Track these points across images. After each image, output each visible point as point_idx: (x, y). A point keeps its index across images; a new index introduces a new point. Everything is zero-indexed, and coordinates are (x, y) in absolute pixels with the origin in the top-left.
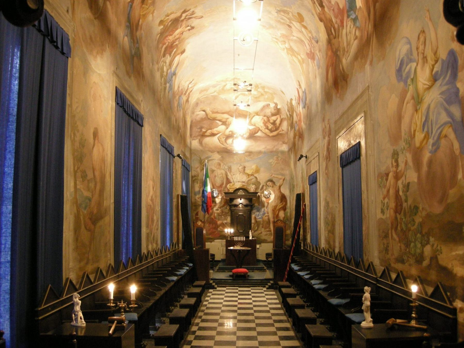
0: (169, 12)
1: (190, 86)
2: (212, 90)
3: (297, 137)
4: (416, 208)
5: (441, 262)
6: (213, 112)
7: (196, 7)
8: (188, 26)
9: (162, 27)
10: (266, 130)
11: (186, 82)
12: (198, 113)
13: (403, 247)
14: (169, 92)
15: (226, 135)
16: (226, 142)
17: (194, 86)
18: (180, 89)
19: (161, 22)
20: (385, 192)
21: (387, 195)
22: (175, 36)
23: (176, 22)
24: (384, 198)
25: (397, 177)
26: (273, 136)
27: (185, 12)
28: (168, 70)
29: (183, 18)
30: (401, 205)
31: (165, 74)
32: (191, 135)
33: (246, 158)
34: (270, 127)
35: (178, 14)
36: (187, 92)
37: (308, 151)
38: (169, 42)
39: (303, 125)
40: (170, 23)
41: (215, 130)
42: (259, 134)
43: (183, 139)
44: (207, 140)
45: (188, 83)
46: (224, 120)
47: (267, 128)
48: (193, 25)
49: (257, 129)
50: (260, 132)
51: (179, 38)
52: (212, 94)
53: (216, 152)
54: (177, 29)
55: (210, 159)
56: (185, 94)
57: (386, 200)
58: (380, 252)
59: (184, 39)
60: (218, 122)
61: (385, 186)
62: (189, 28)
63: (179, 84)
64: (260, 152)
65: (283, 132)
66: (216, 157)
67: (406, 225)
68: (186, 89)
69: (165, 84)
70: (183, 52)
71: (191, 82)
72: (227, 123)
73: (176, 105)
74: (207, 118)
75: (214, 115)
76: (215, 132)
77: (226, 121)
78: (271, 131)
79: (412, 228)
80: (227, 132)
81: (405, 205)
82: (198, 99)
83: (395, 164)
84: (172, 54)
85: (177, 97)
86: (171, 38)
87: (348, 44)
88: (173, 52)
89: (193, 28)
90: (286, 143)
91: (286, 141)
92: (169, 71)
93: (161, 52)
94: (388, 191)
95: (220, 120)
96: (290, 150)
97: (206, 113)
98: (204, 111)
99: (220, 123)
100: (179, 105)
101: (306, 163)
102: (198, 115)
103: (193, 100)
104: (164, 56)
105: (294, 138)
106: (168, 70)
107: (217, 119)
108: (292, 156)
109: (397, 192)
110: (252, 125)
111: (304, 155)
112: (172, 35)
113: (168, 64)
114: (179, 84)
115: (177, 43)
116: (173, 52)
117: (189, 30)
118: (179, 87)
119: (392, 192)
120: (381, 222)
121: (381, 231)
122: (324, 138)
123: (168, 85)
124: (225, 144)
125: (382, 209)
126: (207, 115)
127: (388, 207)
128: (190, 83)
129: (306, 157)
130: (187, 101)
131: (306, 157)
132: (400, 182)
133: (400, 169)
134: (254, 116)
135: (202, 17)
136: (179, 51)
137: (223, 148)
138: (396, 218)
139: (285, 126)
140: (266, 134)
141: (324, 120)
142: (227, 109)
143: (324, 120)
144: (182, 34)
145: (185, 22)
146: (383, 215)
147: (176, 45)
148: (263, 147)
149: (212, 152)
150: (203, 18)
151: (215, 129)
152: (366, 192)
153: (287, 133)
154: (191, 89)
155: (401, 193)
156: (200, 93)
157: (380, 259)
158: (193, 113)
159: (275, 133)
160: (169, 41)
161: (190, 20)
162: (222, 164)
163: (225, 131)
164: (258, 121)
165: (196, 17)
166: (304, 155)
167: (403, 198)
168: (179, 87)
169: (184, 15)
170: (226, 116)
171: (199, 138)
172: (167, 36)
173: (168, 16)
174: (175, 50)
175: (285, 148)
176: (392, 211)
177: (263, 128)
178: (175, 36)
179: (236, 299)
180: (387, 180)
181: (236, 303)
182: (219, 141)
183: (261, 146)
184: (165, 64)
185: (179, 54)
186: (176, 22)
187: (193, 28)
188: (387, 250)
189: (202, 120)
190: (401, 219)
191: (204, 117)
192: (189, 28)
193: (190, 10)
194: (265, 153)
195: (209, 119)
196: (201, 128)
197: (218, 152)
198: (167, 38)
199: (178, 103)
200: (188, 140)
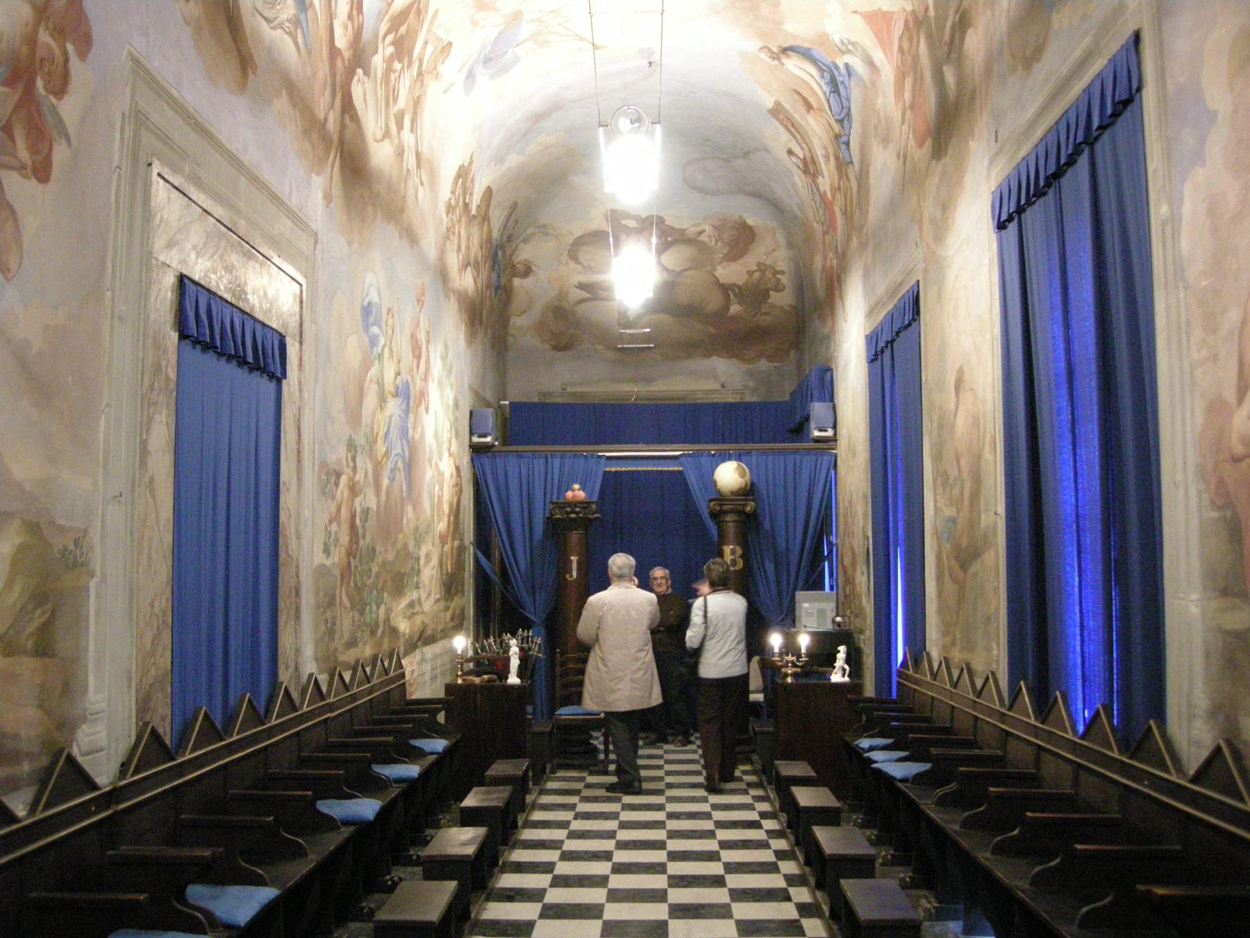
4: (374, 550)
5: (392, 623)
13: (357, 615)
20: (333, 510)
21: (335, 518)
24: (331, 522)
25: (354, 490)
30: (357, 543)
57: (334, 527)
58: (317, 643)
61: (333, 497)
67: (361, 577)
79: (369, 582)
81: (362, 542)
83: (351, 464)
94: (339, 510)
109: (353, 517)
119: (345, 513)
120: (321, 571)
121: (322, 594)
125: (325, 544)
127: (337, 540)
132: (357, 501)
133: (357, 478)
138: (349, 563)
146: (328, 556)
152: (294, 489)
155: (358, 522)
157: (317, 660)
167: (361, 531)
176: (343, 550)
179: (658, 856)
180: (337, 485)
181: (659, 882)
188: (331, 633)
190: (356, 567)
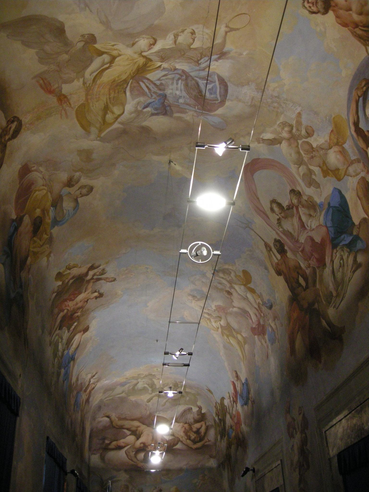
0: (72, 264)
1: (92, 381)
2: (119, 390)
3: (233, 447)
6: (120, 419)
7: (107, 263)
8: (95, 292)
9: (60, 283)
10: (188, 441)
11: (87, 375)
12: (100, 419)
14: (64, 382)
16: (136, 457)
17: (97, 382)
18: (79, 382)
19: (59, 275)
22: (77, 304)
23: (80, 281)
26: (197, 449)
27: (92, 268)
28: (64, 350)
29: (89, 277)
31: (60, 354)
32: (90, 448)
33: (162, 478)
35: (83, 270)
36: (87, 389)
37: (255, 463)
38: (68, 310)
39: (244, 428)
40: (71, 281)
41: (122, 442)
42: (179, 446)
43: (79, 451)
44: (111, 455)
45: (89, 376)
46: (134, 429)
47: (189, 438)
48: (102, 291)
51: (82, 307)
52: (118, 396)
54: (80, 293)
55: (115, 479)
56: (85, 391)
59: (88, 310)
60: (125, 431)
62: (96, 294)
63: (78, 375)
64: (180, 470)
66: (123, 477)
68: (87, 383)
69: (60, 368)
70: (86, 330)
71: (94, 376)
72: (138, 432)
73: (72, 402)
74: (112, 425)
75: (120, 423)
76: (123, 444)
77: (137, 430)
80: (138, 444)
82: (101, 401)
84: (72, 329)
85: (75, 392)
86: (71, 305)
87: (340, 284)
88: (73, 327)
89: (101, 295)
90: (214, 457)
91: (214, 455)
92: (66, 352)
93: (56, 322)
95: (128, 429)
96: (221, 465)
97: (110, 419)
98: (108, 417)
99: (128, 432)
100: (76, 403)
101: (252, 479)
102: (101, 421)
103: (96, 400)
104: (60, 328)
105: (229, 446)
106: (64, 350)
107: (125, 427)
108: (226, 474)
111: (251, 468)
112: (71, 300)
113: (65, 341)
114: (78, 375)
115: (79, 314)
116: (73, 327)
117: (96, 298)
118: (77, 379)
122: (292, 436)
123: (63, 371)
124: (135, 460)
126: (111, 422)
128: (93, 377)
129: (254, 470)
130: (88, 401)
131: (254, 470)
135: (115, 280)
136: (81, 327)
137: (132, 465)
139: (212, 433)
140: (187, 445)
141: (288, 411)
142: (137, 413)
143: (288, 411)
144: (87, 301)
145: (91, 284)
147: (78, 316)
149: (119, 470)
150: (116, 282)
151: (122, 441)
153: (215, 444)
154: (93, 386)
156: (104, 393)
158: (94, 419)
159: (199, 445)
160: (69, 309)
161: (98, 282)
162: (130, 487)
163: (135, 443)
165: (107, 278)
166: (251, 468)
168: (77, 379)
169: (91, 273)
170: (136, 423)
172: (66, 300)
173: (70, 269)
174: (76, 324)
175: (212, 463)
177: (184, 439)
178: (77, 304)
183: (182, 463)
184: (60, 341)
185: (80, 332)
186: (80, 281)
187: (101, 295)
189: (105, 428)
191: (108, 425)
192: (96, 294)
193: (100, 266)
195: (115, 427)
196: (104, 439)
197: (126, 471)
198: (66, 303)
199: (76, 401)
200: (86, 453)
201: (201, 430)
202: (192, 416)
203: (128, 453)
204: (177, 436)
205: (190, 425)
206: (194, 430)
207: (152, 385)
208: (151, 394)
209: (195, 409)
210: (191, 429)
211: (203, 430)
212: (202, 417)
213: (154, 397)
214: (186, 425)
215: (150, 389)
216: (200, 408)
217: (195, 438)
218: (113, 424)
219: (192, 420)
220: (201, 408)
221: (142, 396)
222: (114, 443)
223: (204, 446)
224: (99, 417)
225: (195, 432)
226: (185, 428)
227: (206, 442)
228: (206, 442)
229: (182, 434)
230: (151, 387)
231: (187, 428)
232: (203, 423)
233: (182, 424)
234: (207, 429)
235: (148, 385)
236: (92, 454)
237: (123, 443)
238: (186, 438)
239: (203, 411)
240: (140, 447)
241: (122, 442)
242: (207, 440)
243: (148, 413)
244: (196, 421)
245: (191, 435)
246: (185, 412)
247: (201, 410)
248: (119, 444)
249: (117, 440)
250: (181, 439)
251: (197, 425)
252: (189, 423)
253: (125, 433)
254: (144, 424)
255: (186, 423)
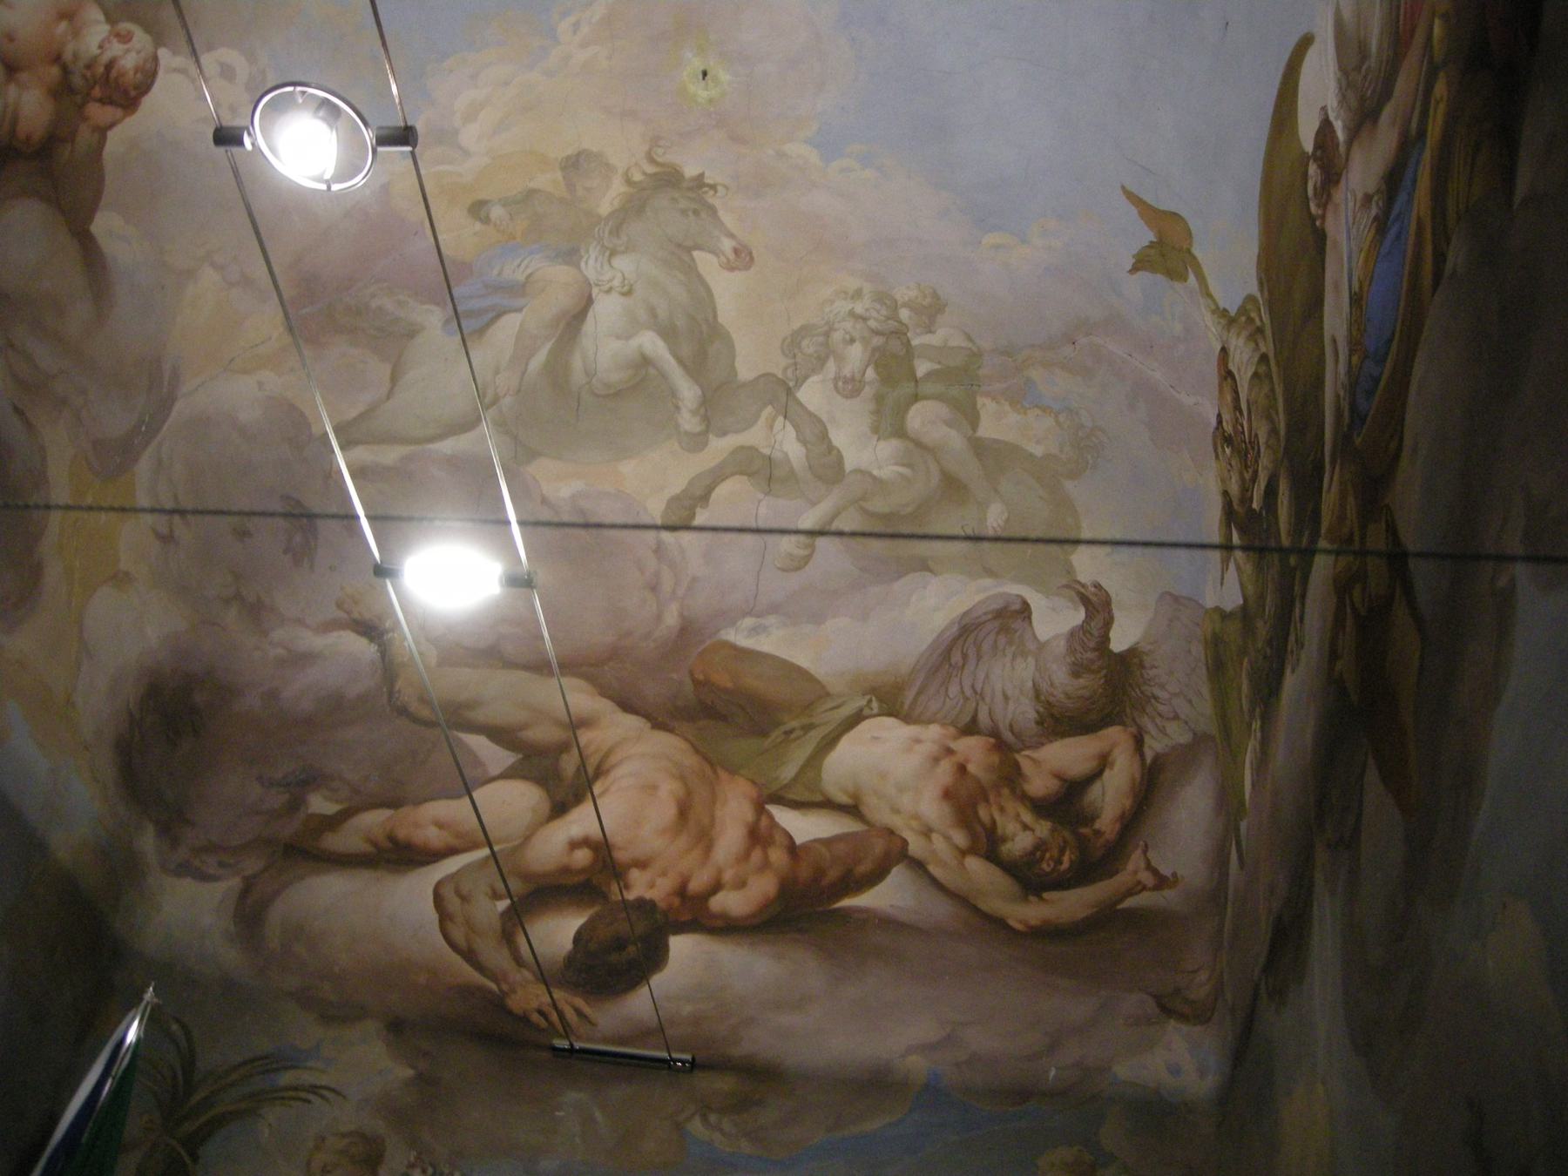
10: (975, 864)
12: (317, 642)
15: (526, 877)
16: (507, 937)
33: (696, 1127)
34: (1019, 842)
41: (432, 818)
42: (890, 895)
44: (329, 900)
46: (542, 734)
47: (988, 844)
49: (879, 846)
50: (898, 876)
53: (371, 1026)
55: (286, 1078)
60: (478, 743)
64: (875, 1084)
65: (1167, 899)
66: (365, 1068)
72: (569, 764)
76: (433, 836)
78: (1029, 877)
90: (1198, 1015)
91: (1200, 987)
99: (495, 757)
102: (303, 659)
107: (479, 716)
110: (828, 804)
124: (497, 957)
134: (857, 719)
140: (960, 899)
148: (924, 1029)
149: (339, 1014)
162: (397, 1157)
163: (527, 839)
164: (891, 765)
171: (252, 865)
177: (942, 846)
182: (444, 916)
194: (932, 1094)
195: (403, 711)
197: (396, 1027)
201: (1095, 791)
202: (1025, 671)
203: (453, 904)
204: (881, 815)
205: (1004, 747)
206: (1039, 784)
207: (700, 340)
208: (697, 442)
209: (1055, 620)
210: (1011, 776)
211: (1110, 797)
212: (1111, 688)
213: (717, 476)
214: (973, 750)
215: (688, 392)
216: (1097, 606)
217: (1041, 846)
218: (399, 684)
219: (1024, 712)
220: (1107, 603)
221: (627, 468)
222: (374, 820)
223: (1107, 919)
224: (300, 622)
225: (1042, 807)
226: (962, 769)
227: (1137, 888)
228: (1137, 888)
229: (931, 808)
230: (696, 367)
231: (971, 768)
232: (1116, 737)
233: (933, 732)
234: (1151, 786)
235: (668, 333)
236: (183, 870)
237: (440, 825)
238: (960, 838)
239: (1120, 641)
240: (566, 870)
241: (432, 818)
242: (1147, 878)
243: (671, 619)
244: (1061, 722)
245: (1007, 826)
246: (965, 641)
247: (1108, 623)
248: (402, 834)
249: (394, 804)
250: (916, 846)
251: (1067, 755)
252: (994, 733)
253: (477, 762)
254: (627, 706)
255: (970, 729)
